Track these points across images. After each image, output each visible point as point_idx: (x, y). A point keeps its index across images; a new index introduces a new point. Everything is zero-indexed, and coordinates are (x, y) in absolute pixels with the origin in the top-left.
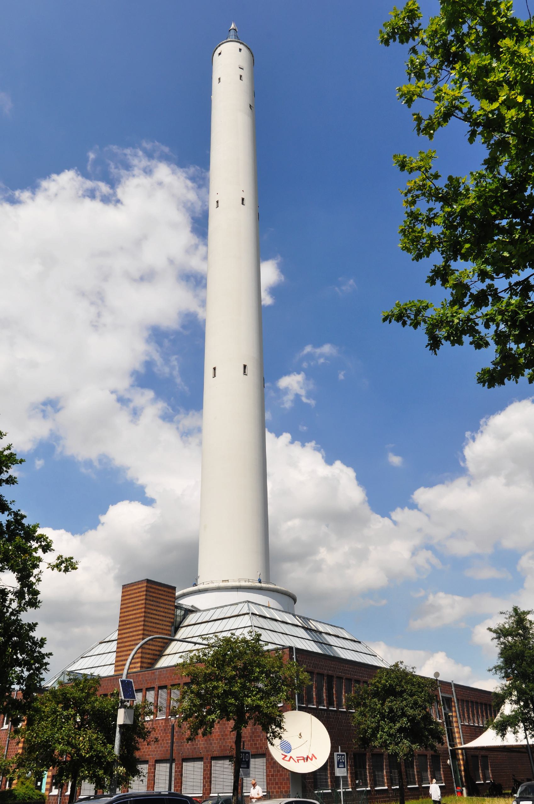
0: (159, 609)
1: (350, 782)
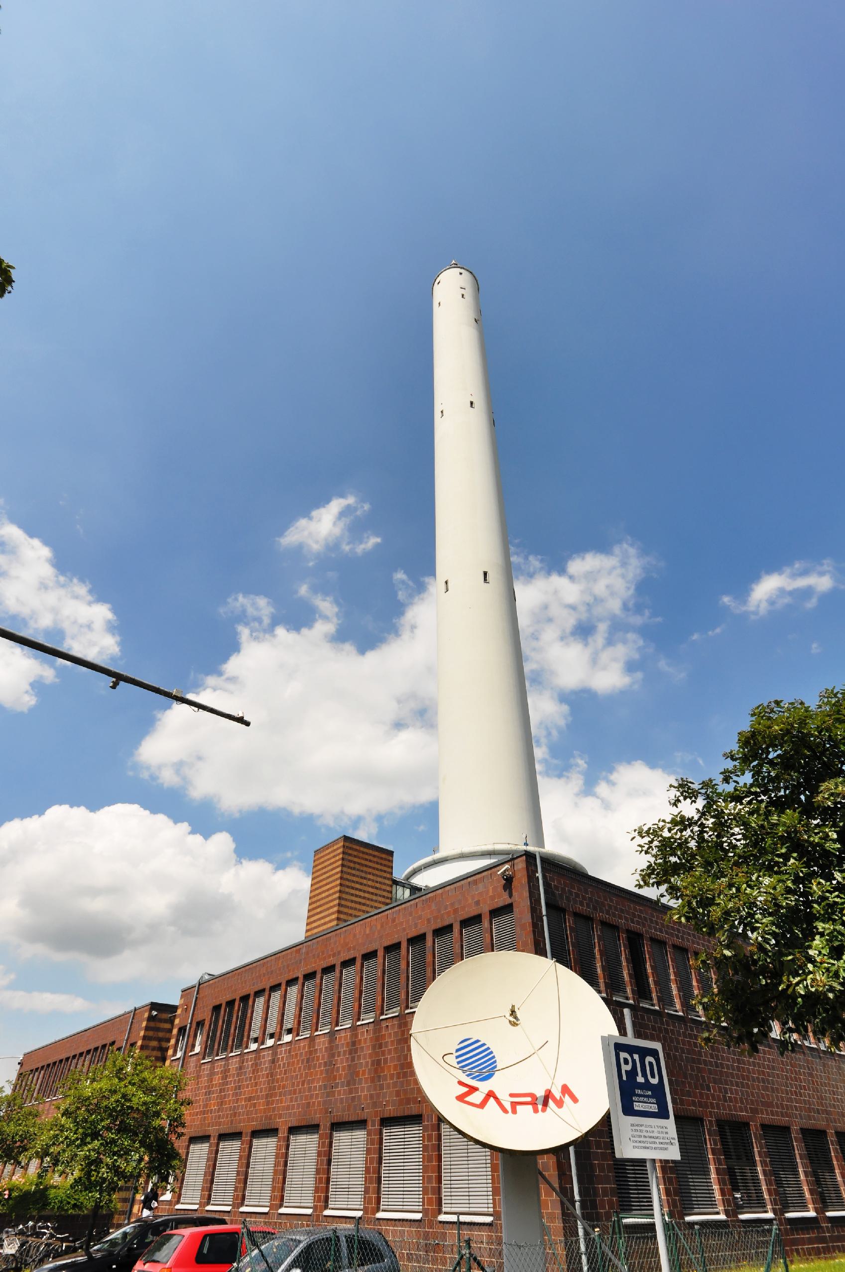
0: (365, 882)
1: (718, 1196)
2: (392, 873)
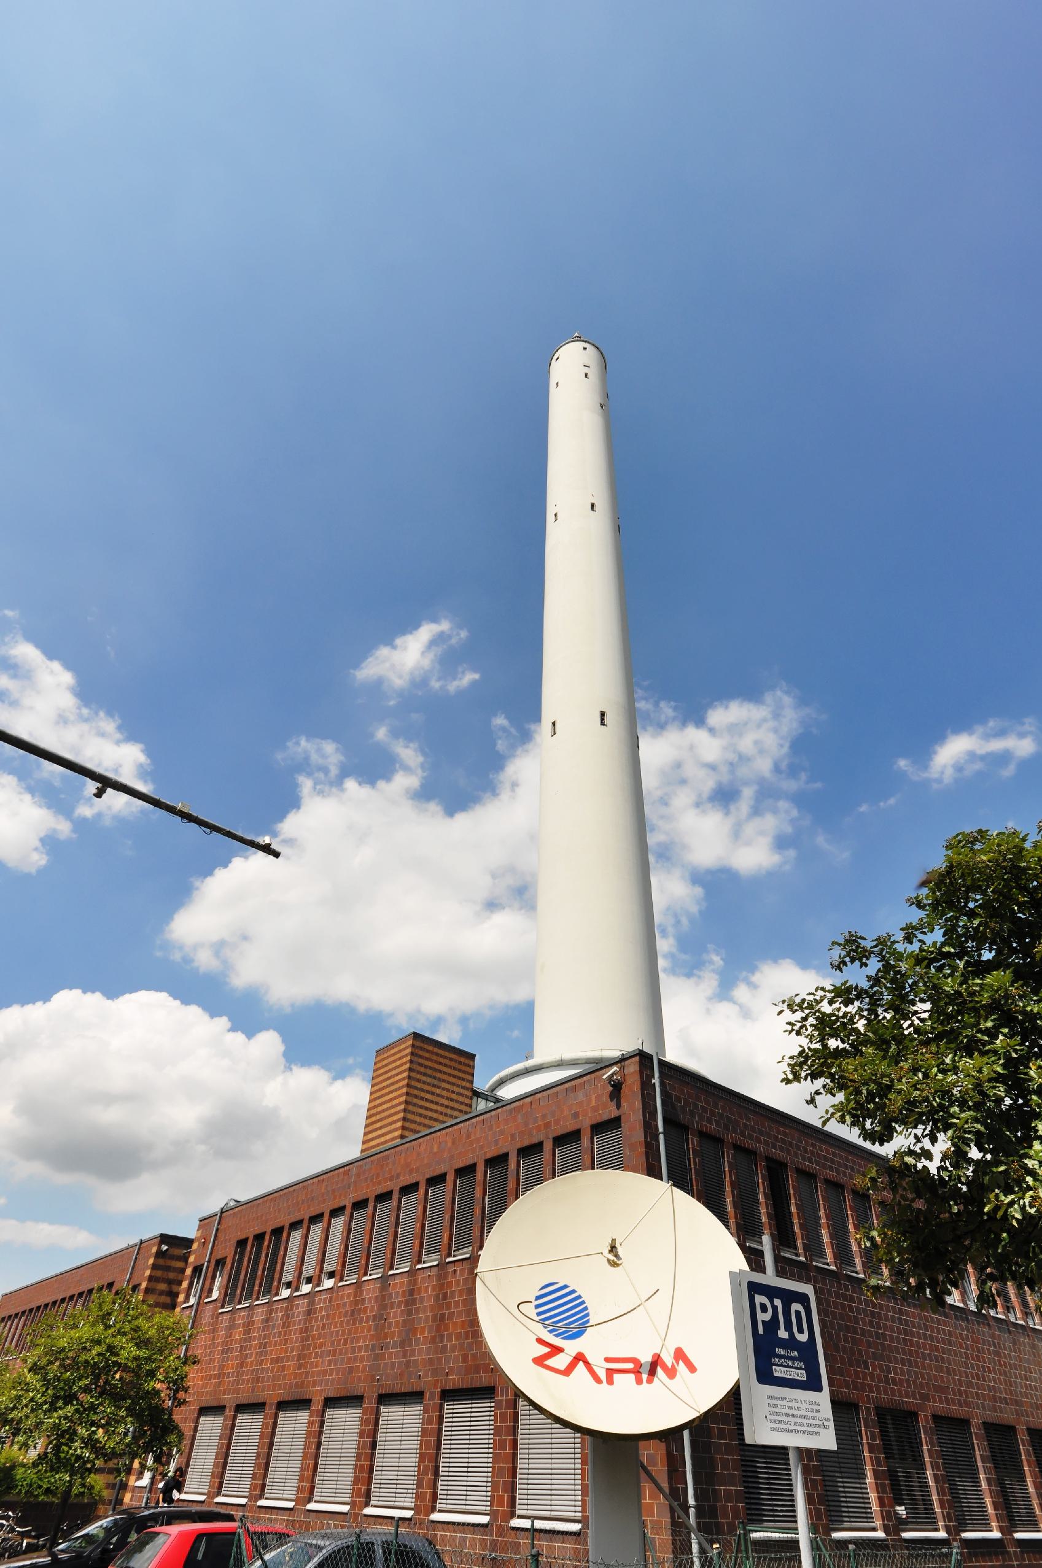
0: (438, 1091)
1: (875, 1507)
2: (472, 1082)
